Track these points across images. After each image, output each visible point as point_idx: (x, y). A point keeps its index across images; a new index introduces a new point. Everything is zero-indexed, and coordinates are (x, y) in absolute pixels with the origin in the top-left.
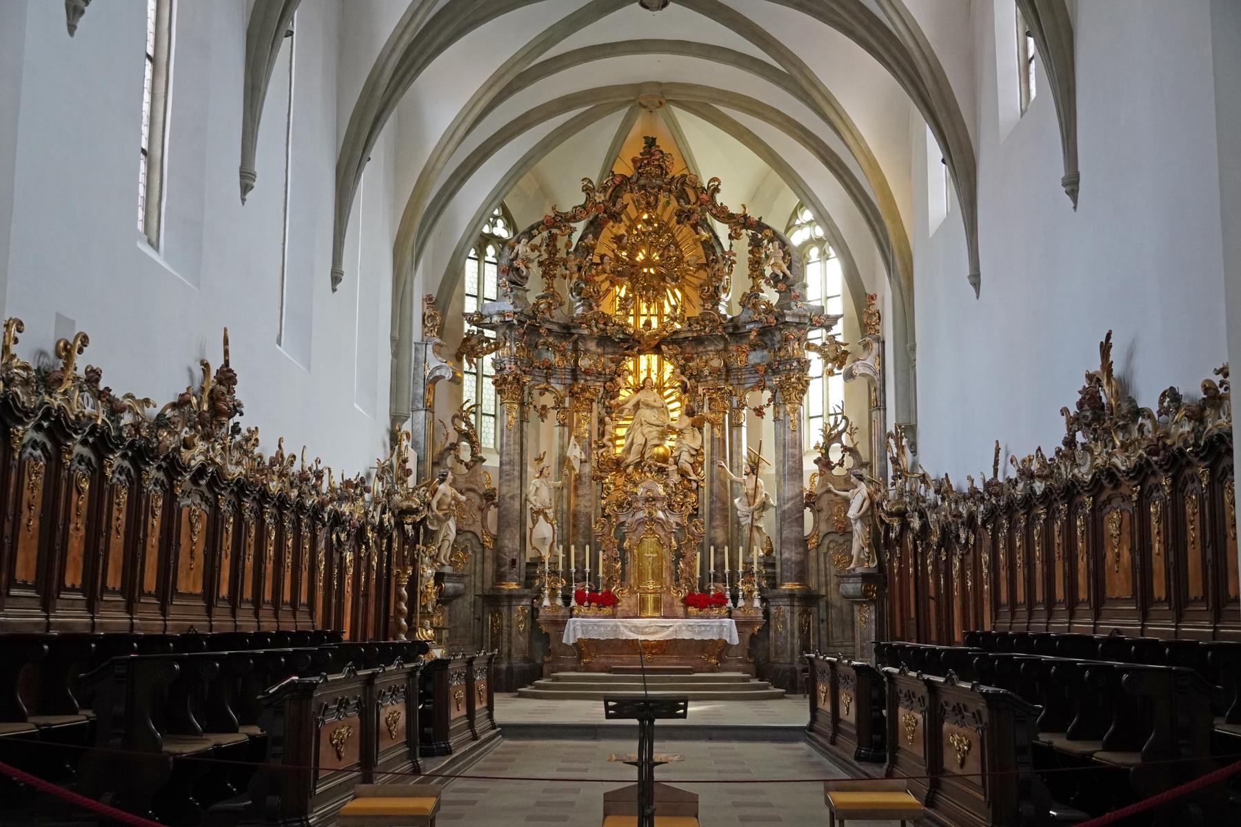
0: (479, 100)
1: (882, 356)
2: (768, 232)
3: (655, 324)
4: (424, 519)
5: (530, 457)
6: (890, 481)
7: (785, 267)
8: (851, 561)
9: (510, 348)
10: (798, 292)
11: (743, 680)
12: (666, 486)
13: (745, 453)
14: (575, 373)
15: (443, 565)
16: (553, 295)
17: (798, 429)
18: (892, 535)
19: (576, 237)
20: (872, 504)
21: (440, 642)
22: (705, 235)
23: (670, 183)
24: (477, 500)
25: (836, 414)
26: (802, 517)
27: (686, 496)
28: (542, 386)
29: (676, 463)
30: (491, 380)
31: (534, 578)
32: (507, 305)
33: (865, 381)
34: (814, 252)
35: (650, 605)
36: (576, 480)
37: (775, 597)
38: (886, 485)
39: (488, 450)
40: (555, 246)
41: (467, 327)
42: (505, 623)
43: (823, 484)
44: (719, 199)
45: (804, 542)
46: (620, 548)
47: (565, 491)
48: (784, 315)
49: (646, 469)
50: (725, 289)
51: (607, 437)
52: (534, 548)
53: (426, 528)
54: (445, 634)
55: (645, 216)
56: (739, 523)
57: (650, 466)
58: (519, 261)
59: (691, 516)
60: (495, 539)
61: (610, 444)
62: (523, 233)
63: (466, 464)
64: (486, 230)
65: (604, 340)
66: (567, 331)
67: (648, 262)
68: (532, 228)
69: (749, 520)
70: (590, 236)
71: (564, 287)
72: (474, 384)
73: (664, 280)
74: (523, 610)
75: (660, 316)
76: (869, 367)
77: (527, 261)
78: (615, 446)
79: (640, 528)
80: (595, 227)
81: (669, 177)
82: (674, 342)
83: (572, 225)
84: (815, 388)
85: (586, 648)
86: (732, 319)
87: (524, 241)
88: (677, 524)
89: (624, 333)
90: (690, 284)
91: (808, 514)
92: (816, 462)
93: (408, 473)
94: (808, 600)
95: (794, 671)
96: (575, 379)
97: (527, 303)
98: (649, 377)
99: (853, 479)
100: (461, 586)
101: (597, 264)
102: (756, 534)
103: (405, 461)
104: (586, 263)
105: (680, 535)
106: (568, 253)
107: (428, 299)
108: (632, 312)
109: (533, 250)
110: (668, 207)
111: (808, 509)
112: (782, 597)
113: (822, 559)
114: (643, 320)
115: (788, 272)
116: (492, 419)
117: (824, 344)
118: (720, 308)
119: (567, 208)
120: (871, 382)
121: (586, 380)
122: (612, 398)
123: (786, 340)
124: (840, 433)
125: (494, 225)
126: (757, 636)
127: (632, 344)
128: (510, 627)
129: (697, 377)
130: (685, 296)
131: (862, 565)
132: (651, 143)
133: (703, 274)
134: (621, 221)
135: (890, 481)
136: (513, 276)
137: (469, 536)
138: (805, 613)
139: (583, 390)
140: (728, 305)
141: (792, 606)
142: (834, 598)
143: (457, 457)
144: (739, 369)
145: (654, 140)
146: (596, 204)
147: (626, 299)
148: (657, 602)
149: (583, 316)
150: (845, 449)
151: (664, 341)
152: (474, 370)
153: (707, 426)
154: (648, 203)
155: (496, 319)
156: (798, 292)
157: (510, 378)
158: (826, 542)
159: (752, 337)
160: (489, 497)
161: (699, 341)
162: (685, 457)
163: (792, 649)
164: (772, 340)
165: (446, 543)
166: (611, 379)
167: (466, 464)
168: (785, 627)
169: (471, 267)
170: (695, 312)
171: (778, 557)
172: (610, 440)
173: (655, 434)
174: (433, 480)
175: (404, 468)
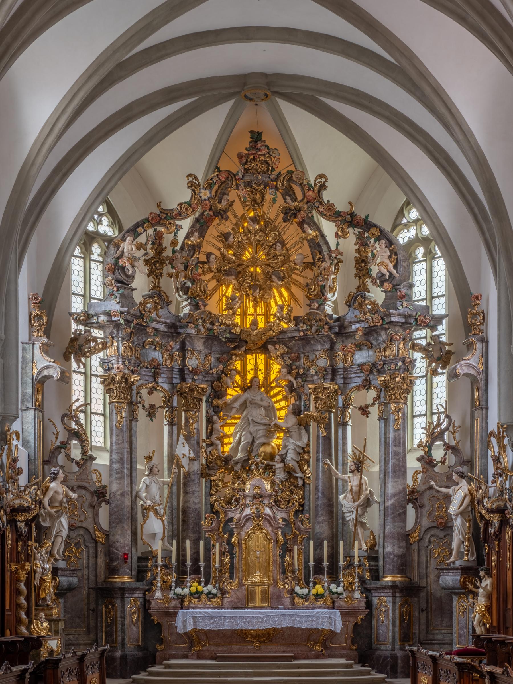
0: (79, 90)
1: (485, 356)
2: (375, 231)
3: (261, 325)
4: (37, 516)
5: (141, 453)
6: (491, 478)
7: (391, 266)
8: (450, 554)
9: (118, 348)
10: (404, 291)
11: (347, 666)
12: (273, 483)
13: (349, 450)
16: (159, 295)
17: (401, 429)
18: (492, 530)
19: (181, 235)
21: (56, 632)
22: (311, 233)
23: (276, 180)
24: (88, 497)
25: (439, 413)
26: (405, 513)
27: (292, 492)
30: (99, 380)
31: (146, 571)
32: (114, 305)
33: (468, 381)
34: (420, 252)
35: (258, 596)
36: (185, 477)
37: (377, 589)
38: (486, 482)
39: (98, 448)
40: (160, 244)
41: (74, 326)
42: (118, 614)
43: (425, 481)
44: (326, 196)
45: (405, 537)
47: (175, 488)
48: (389, 315)
50: (331, 289)
51: (214, 436)
52: (144, 543)
53: (39, 527)
54: (61, 625)
55: (252, 214)
56: (343, 518)
57: (257, 464)
58: (125, 259)
61: (218, 442)
62: (128, 231)
63: (77, 463)
64: (91, 227)
66: (175, 328)
67: (254, 262)
68: (138, 225)
69: (354, 516)
70: (196, 234)
72: (82, 383)
74: (135, 602)
75: (267, 315)
76: (473, 367)
78: (223, 444)
80: (201, 226)
81: (275, 173)
82: (281, 341)
83: (178, 222)
84: (419, 388)
86: (338, 320)
87: (129, 239)
88: (284, 520)
89: (230, 332)
90: (296, 283)
91: (411, 510)
92: (419, 460)
93: (19, 472)
95: (394, 657)
97: (133, 303)
99: (455, 477)
100: (75, 580)
101: (204, 263)
102: (360, 530)
103: (15, 460)
104: (193, 262)
106: (174, 252)
108: (239, 311)
109: (138, 248)
110: (273, 206)
111: (410, 505)
112: (384, 588)
114: (249, 319)
115: (394, 271)
116: (102, 418)
117: (429, 344)
118: (326, 307)
119: (172, 205)
120: (474, 381)
121: (193, 379)
124: (442, 432)
125: (100, 223)
127: (237, 343)
128: (123, 618)
130: (292, 295)
131: (461, 558)
132: (256, 137)
133: (309, 273)
134: (227, 219)
135: (491, 478)
137: (82, 532)
140: (333, 303)
141: (394, 596)
143: (68, 456)
145: (260, 134)
146: (201, 202)
147: (233, 298)
148: (264, 593)
149: (189, 316)
150: (448, 447)
151: (271, 341)
152: (82, 370)
153: (312, 426)
154: (254, 201)
155: (103, 318)
156: (404, 291)
157: (118, 378)
159: (357, 337)
160: (100, 494)
161: (305, 340)
162: (291, 456)
164: (377, 340)
165: (59, 540)
168: (387, 617)
169: (76, 266)
170: (300, 312)
171: (381, 551)
172: (218, 439)
174: (44, 478)
175: (14, 468)
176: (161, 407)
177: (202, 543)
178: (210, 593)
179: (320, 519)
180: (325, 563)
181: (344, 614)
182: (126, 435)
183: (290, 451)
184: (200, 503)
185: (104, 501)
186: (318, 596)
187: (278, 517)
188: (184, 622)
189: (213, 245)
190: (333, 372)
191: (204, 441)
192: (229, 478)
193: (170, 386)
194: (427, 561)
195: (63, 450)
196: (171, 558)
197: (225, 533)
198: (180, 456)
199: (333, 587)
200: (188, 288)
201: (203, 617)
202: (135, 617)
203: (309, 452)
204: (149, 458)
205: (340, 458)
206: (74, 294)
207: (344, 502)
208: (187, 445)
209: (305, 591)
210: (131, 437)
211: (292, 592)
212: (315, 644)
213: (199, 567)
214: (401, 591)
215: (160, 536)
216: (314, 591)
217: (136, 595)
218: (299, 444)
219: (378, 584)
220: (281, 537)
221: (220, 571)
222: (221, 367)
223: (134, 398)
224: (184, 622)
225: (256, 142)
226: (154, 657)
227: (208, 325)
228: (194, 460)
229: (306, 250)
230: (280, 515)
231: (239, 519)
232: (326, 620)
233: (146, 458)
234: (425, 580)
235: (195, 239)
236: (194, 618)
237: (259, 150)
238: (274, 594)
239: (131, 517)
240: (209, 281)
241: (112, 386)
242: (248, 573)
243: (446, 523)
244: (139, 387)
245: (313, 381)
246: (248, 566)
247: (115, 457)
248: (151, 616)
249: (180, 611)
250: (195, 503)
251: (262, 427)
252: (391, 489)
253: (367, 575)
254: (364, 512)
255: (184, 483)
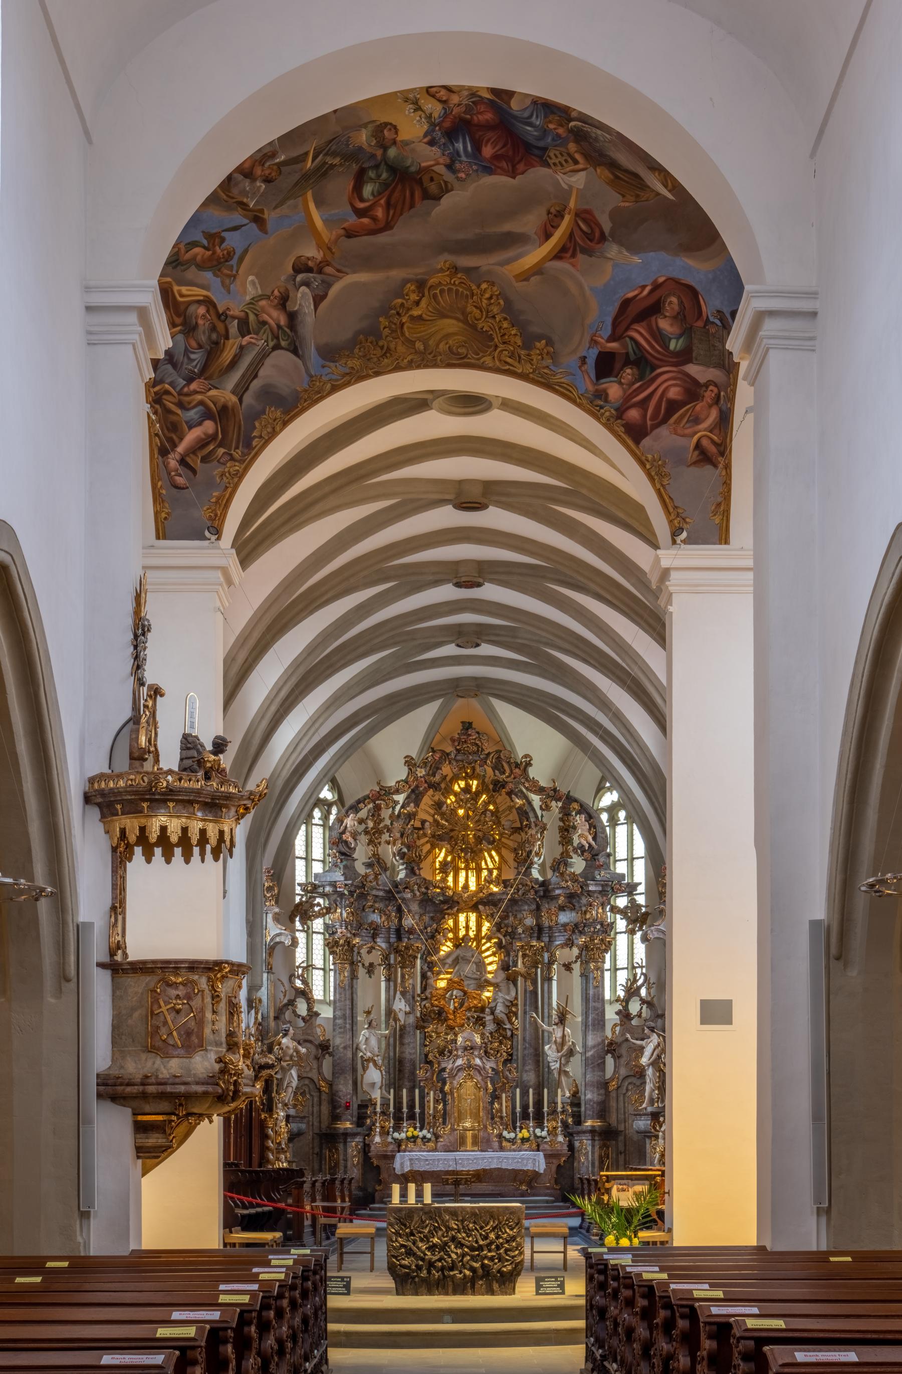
12: (483, 1036)
24: (313, 1050)
26: (604, 1063)
29: (492, 1013)
31: (365, 1118)
35: (469, 1140)
36: (401, 1030)
37: (579, 1133)
42: (341, 1157)
43: (622, 1034)
45: (604, 1085)
47: (392, 1040)
50: (537, 854)
52: (364, 1092)
56: (549, 1067)
59: (506, 1062)
60: (330, 1085)
63: (303, 1019)
69: (558, 1065)
74: (356, 1146)
79: (460, 1074)
88: (493, 1069)
91: (610, 1061)
96: (399, 938)
101: (419, 829)
102: (563, 1079)
111: (609, 1055)
112: (584, 1132)
121: (409, 939)
124: (639, 988)
127: (451, 904)
128: (346, 1160)
137: (307, 1082)
141: (593, 1140)
143: (294, 1012)
148: (475, 1137)
151: (481, 902)
160: (324, 1047)
162: (500, 1009)
164: (579, 902)
168: (587, 1159)
171: (583, 1097)
176: (379, 965)
177: (417, 1091)
178: (424, 1137)
179: (527, 1068)
180: (531, 1109)
181: (547, 1156)
182: (348, 993)
183: (499, 1004)
184: (415, 1053)
185: (328, 1053)
186: (524, 1140)
187: (488, 1067)
188: (402, 1164)
189: (427, 812)
190: (539, 931)
191: (419, 996)
192: (442, 1028)
193: (387, 945)
194: (624, 1107)
195: (290, 1007)
196: (389, 1105)
197: (438, 1082)
198: (397, 1011)
199: (538, 1132)
200: (404, 854)
201: (419, 1160)
202: (356, 1160)
203: (517, 1005)
204: (368, 1013)
205: (546, 1011)
206: (298, 858)
207: (549, 1052)
208: (403, 1000)
209: (512, 1135)
210: (352, 993)
211: (500, 1136)
212: (521, 1183)
213: (414, 1114)
214: (600, 1134)
215: (379, 1084)
216: (520, 1135)
217: (357, 1140)
218: (508, 998)
219: (580, 1128)
220: (490, 1086)
221: (434, 1117)
222: (435, 926)
223: (355, 958)
224: (402, 1164)
225: (467, 729)
226: (374, 1197)
227: (423, 890)
228: (410, 1013)
229: (514, 816)
230: (489, 1065)
231: (452, 1069)
232: (530, 1161)
233: (365, 1012)
234: (623, 1125)
235: (411, 808)
236: (411, 1160)
237: (470, 735)
238: (484, 1138)
239: (353, 1068)
240: (423, 845)
241: (335, 949)
242: (460, 1119)
243: (641, 1072)
244: (360, 947)
245: (520, 939)
246: (459, 1112)
247: (338, 1013)
248: (370, 1159)
249: (398, 1154)
250: (410, 1054)
251: (473, 982)
252: (591, 1042)
253: (570, 1120)
254: (568, 1062)
255: (400, 1035)
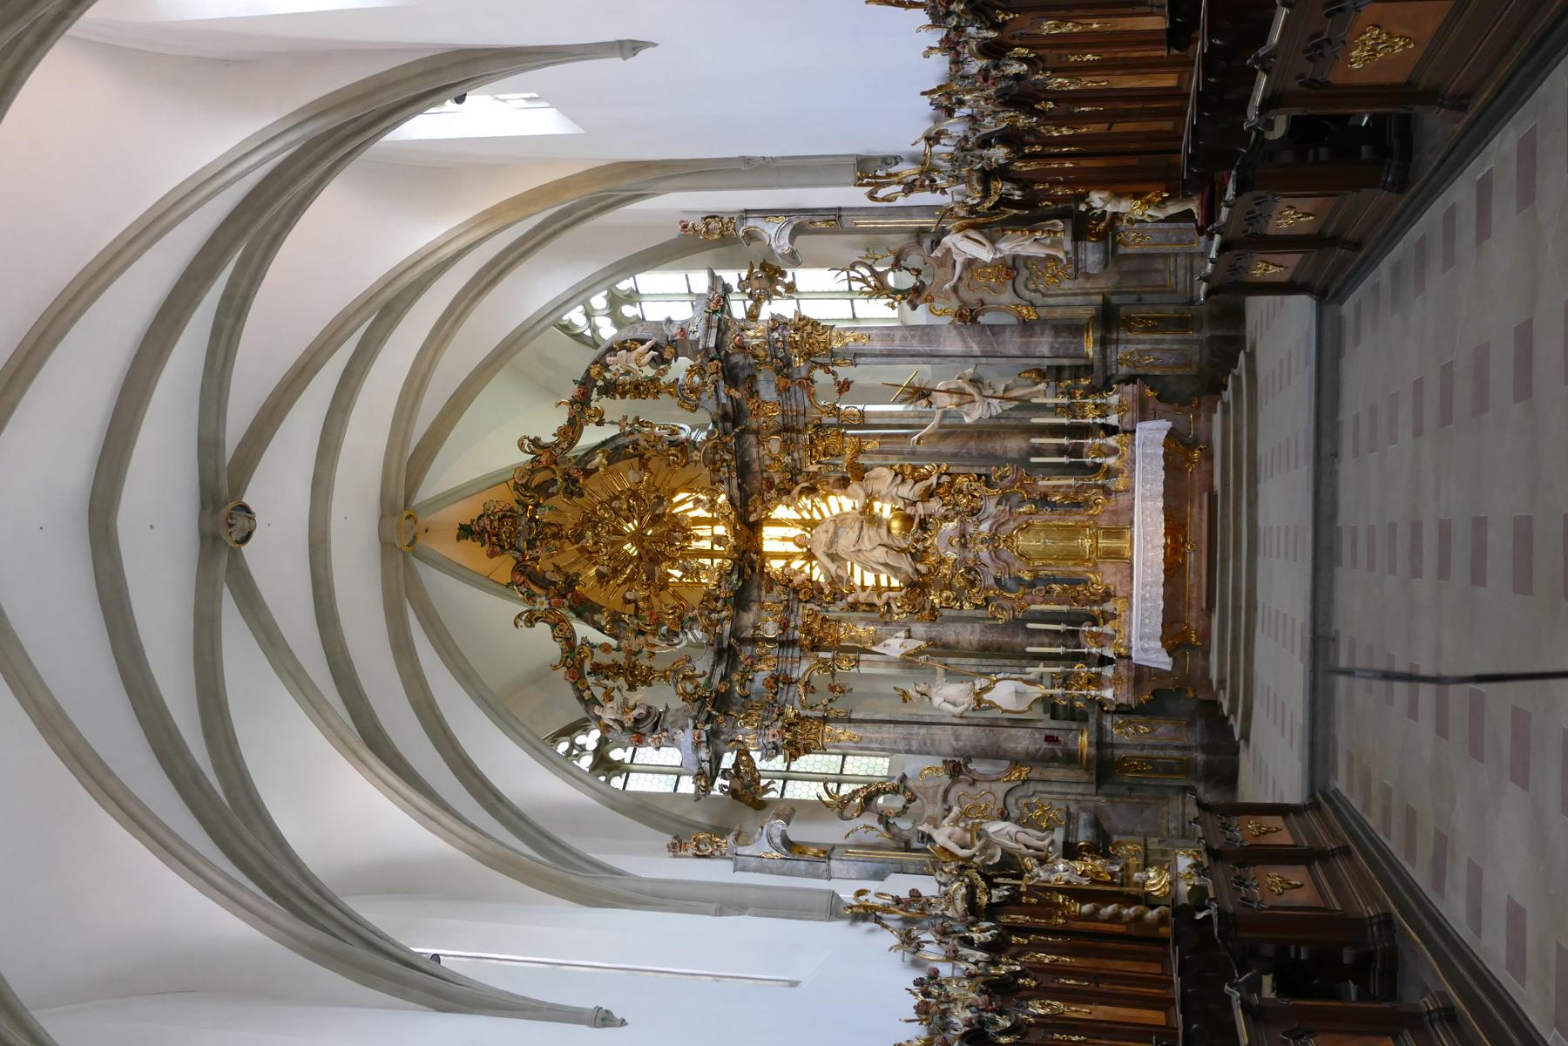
1: (766, 213)
2: (594, 371)
3: (720, 530)
7: (641, 348)
11: (1225, 412)
12: (946, 518)
14: (785, 643)
15: (1052, 843)
17: (868, 334)
19: (597, 637)
20: (974, 226)
22: (599, 459)
26: (991, 327)
27: (960, 491)
28: (802, 691)
29: (914, 503)
33: (800, 239)
35: (1114, 543)
37: (1105, 366)
40: (608, 667)
42: (1137, 753)
44: (548, 438)
46: (1032, 585)
49: (920, 546)
50: (674, 432)
51: (876, 600)
52: (1030, 708)
56: (998, 417)
57: (917, 541)
59: (988, 484)
60: (1016, 762)
61: (885, 596)
63: (909, 801)
64: (586, 762)
65: (740, 601)
68: (581, 698)
69: (995, 402)
70: (596, 617)
71: (665, 652)
72: (799, 783)
73: (660, 516)
74: (1119, 727)
76: (780, 230)
77: (626, 708)
79: (1004, 556)
80: (585, 610)
81: (516, 507)
82: (744, 504)
83: (579, 642)
84: (812, 310)
85: (1175, 635)
86: (715, 423)
88: (999, 503)
92: (914, 308)
94: (1109, 319)
98: (793, 540)
99: (938, 253)
100: (1083, 817)
101: (637, 608)
105: (1015, 500)
106: (619, 649)
107: (676, 847)
111: (980, 319)
112: (1104, 356)
113: (1051, 301)
115: (649, 344)
116: (848, 759)
117: (751, 296)
119: (554, 650)
121: (795, 628)
122: (821, 591)
123: (742, 347)
126: (1160, 394)
128: (1143, 747)
129: (794, 473)
131: (1060, 242)
132: (466, 532)
136: (646, 728)
138: (1127, 323)
139: (809, 632)
140: (693, 428)
141: (1117, 342)
142: (1104, 284)
144: (783, 414)
145: (462, 527)
146: (551, 610)
147: (685, 570)
148: (1109, 533)
149: (705, 630)
151: (742, 517)
153: (862, 460)
157: (788, 736)
158: (1027, 294)
159: (737, 395)
161: (744, 470)
162: (908, 491)
163: (1182, 342)
164: (743, 367)
166: (799, 591)
167: (909, 801)
171: (1048, 362)
172: (879, 596)
173: (872, 533)
176: (833, 675)
181: (1143, 418)
190: (787, 429)
198: (903, 651)
202: (1143, 729)
212: (1190, 460)
219: (1097, 365)
223: (819, 714)
227: (719, 604)
230: (991, 507)
235: (602, 619)
248: (1141, 704)
253: (1084, 382)
